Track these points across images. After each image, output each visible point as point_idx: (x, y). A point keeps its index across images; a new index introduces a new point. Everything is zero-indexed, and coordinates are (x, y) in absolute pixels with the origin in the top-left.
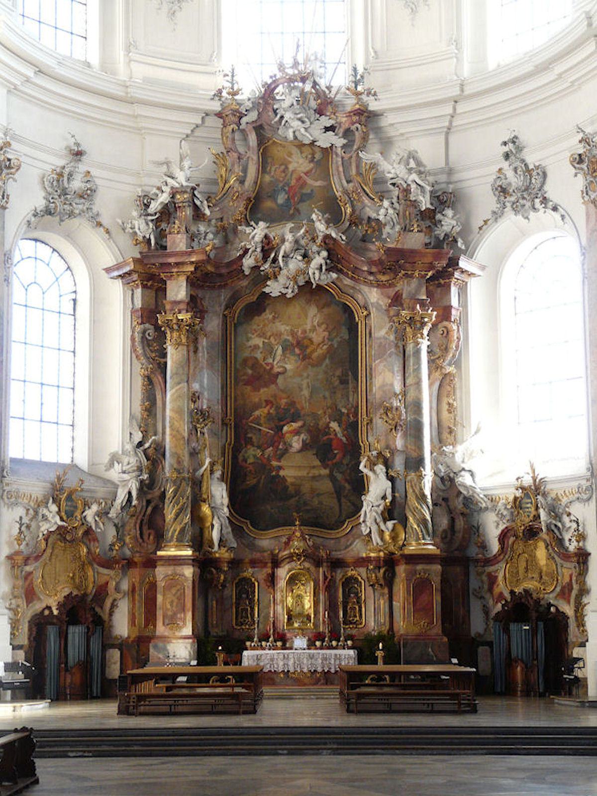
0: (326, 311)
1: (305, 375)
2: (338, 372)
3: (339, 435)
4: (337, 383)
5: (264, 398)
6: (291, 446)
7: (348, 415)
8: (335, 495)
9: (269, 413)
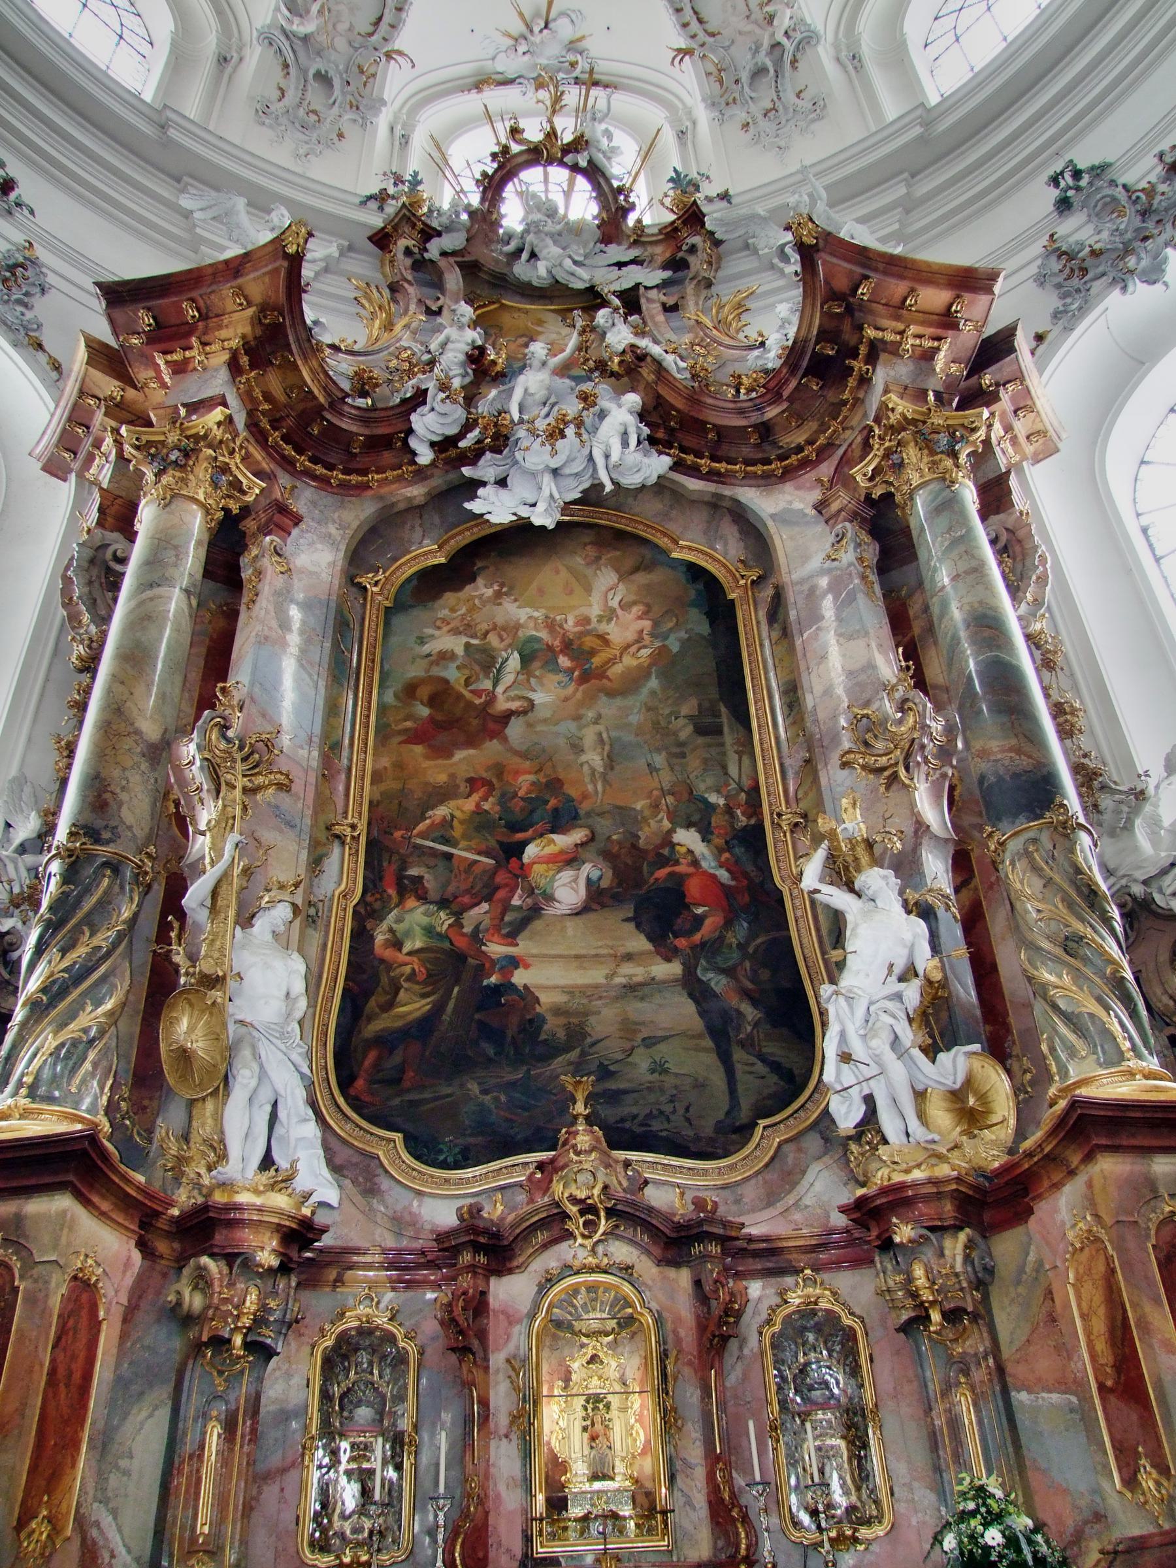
0: (642, 578)
1: (591, 714)
2: (689, 707)
3: (704, 864)
4: (686, 732)
5: (464, 772)
6: (550, 898)
8: (708, 1043)
9: (479, 812)
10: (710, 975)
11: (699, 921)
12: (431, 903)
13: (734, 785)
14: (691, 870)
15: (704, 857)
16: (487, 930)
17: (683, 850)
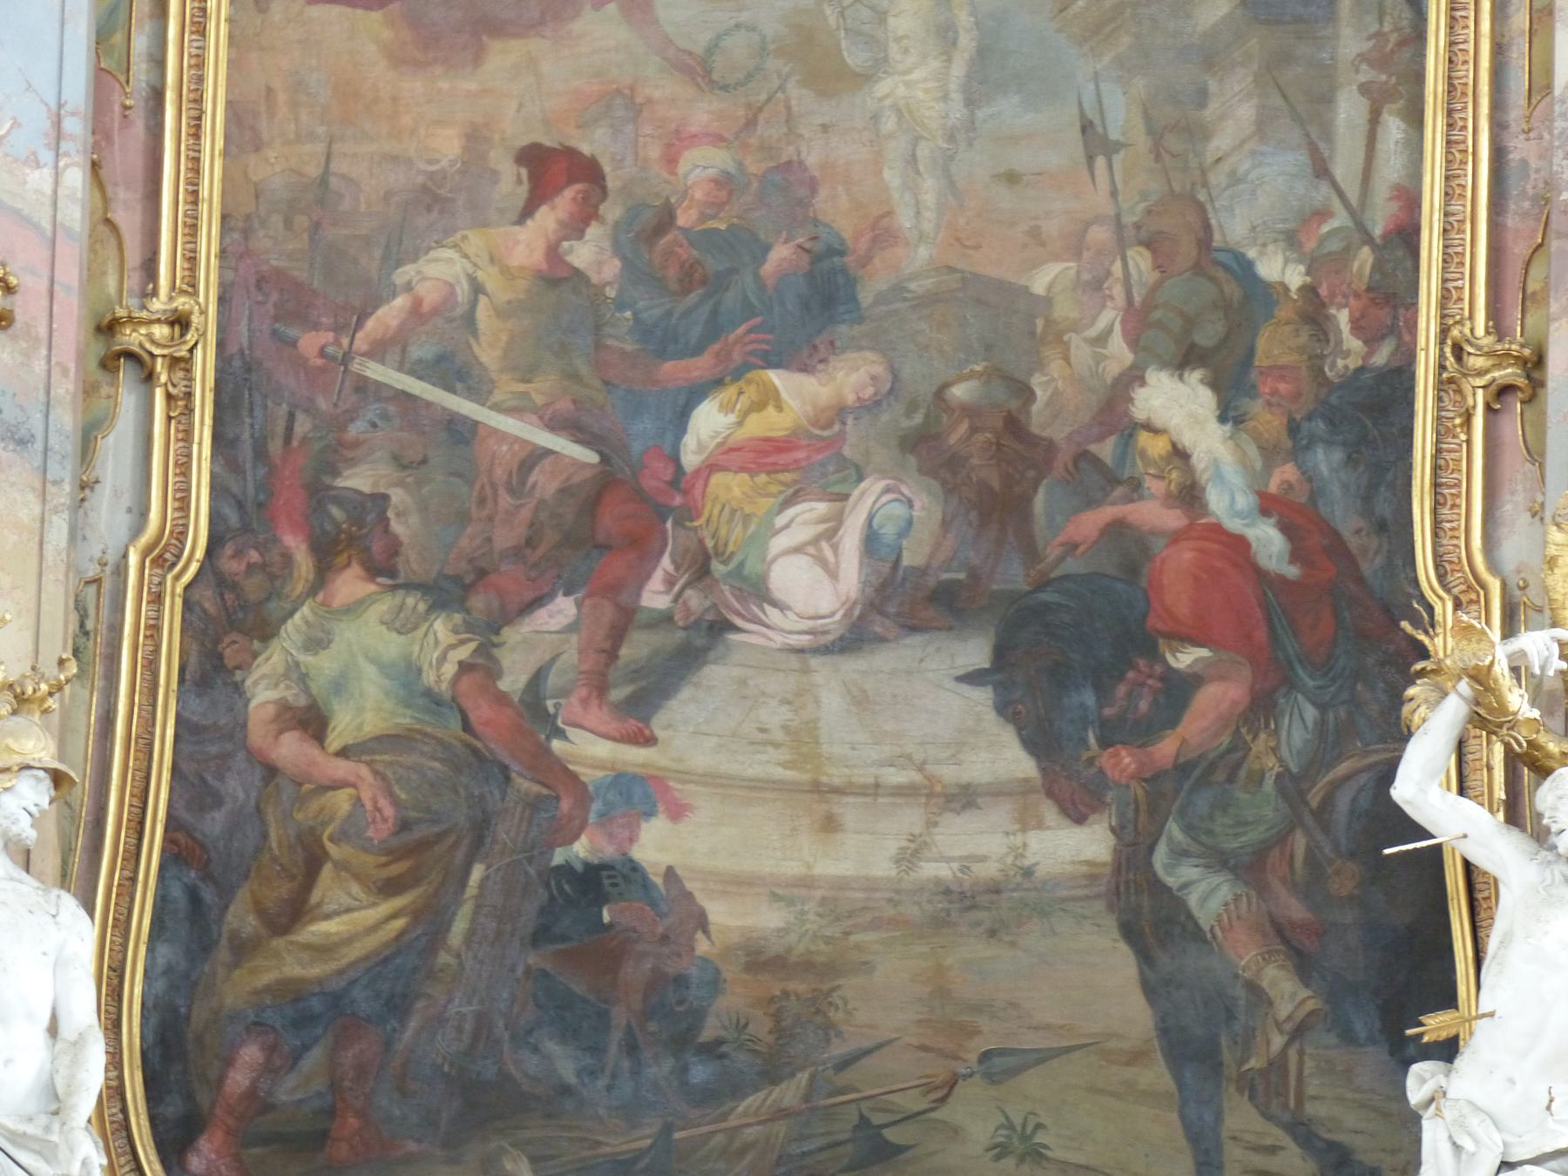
6: (758, 591)
7: (1313, 311)
8: (1157, 1075)
10: (1188, 871)
11: (1179, 689)
12: (409, 587)
13: (1340, 219)
14: (1173, 519)
15: (1219, 477)
16: (564, 692)
17: (1156, 447)
